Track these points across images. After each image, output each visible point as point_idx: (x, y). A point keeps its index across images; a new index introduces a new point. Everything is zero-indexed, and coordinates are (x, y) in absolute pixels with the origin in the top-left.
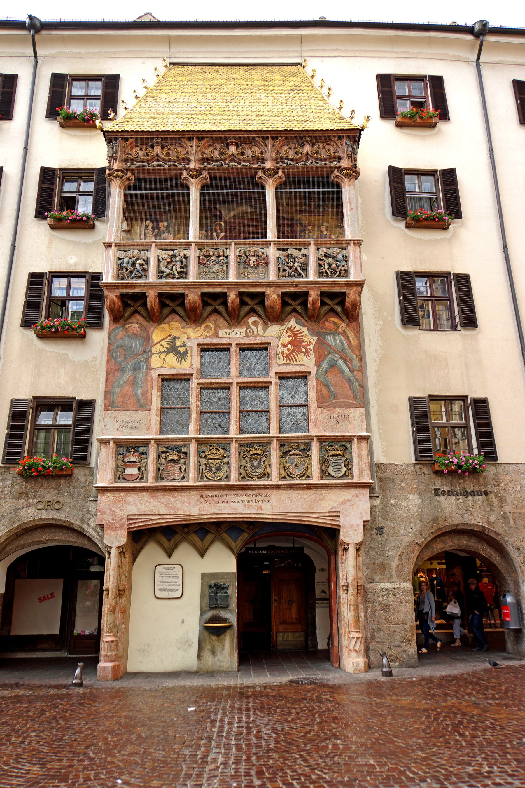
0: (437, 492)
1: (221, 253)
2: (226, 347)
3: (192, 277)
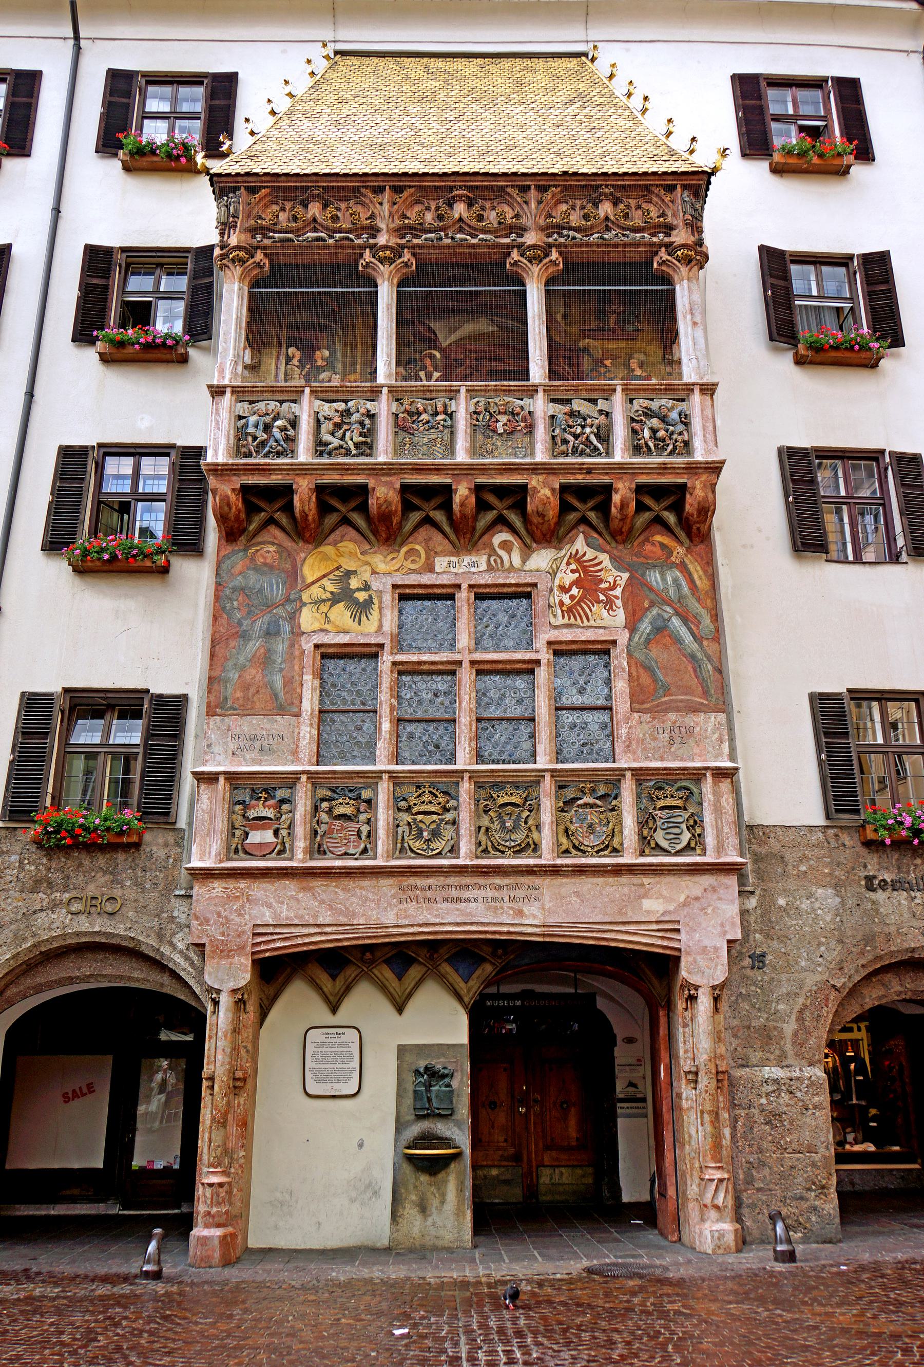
0: (870, 884)
1: (440, 408)
3: (383, 455)
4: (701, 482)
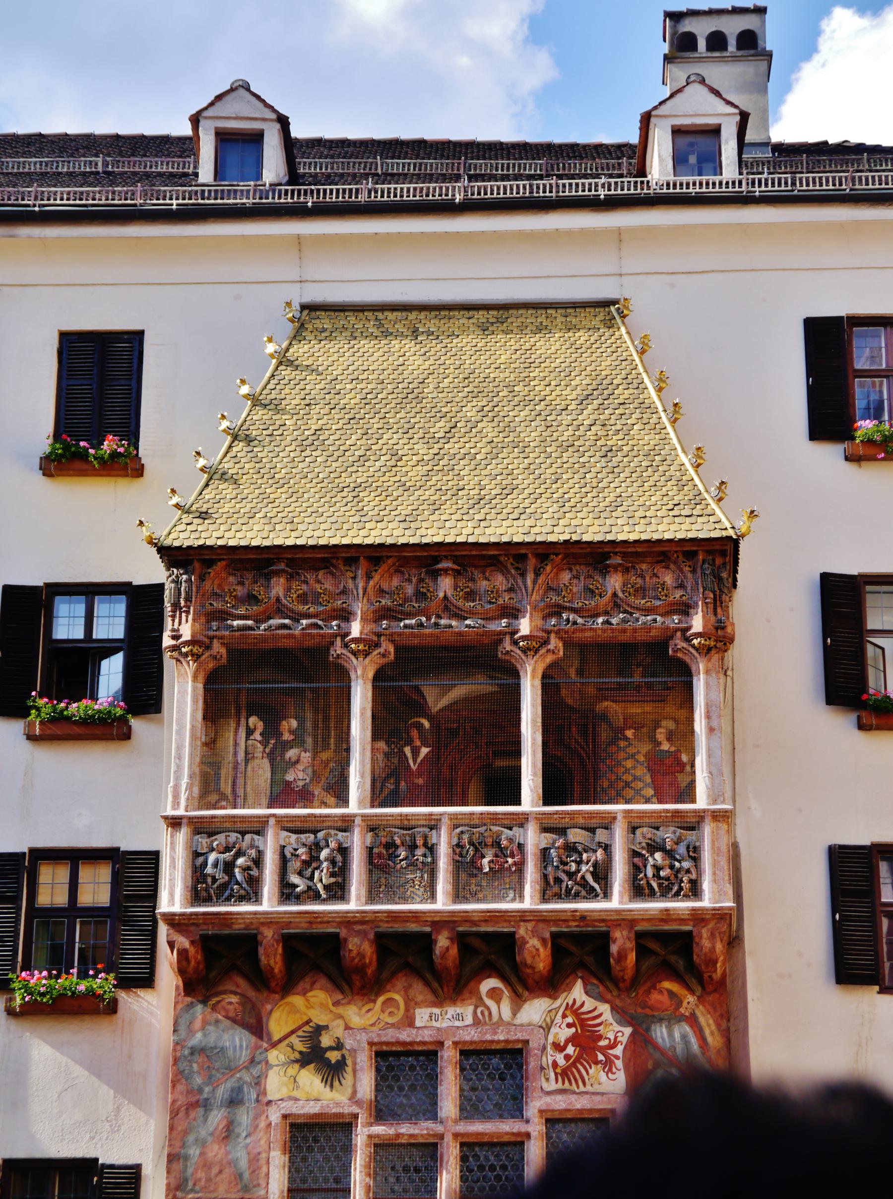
2: (431, 1047)
4: (708, 930)
